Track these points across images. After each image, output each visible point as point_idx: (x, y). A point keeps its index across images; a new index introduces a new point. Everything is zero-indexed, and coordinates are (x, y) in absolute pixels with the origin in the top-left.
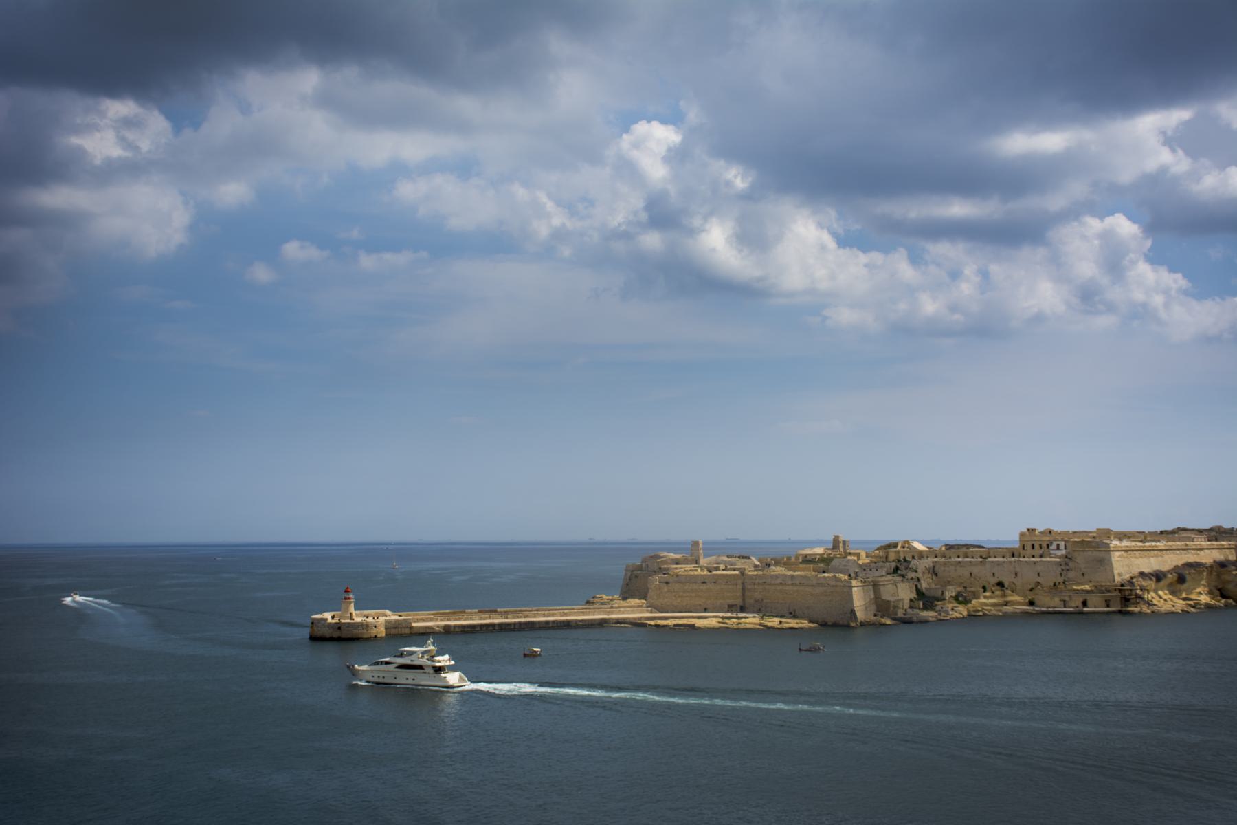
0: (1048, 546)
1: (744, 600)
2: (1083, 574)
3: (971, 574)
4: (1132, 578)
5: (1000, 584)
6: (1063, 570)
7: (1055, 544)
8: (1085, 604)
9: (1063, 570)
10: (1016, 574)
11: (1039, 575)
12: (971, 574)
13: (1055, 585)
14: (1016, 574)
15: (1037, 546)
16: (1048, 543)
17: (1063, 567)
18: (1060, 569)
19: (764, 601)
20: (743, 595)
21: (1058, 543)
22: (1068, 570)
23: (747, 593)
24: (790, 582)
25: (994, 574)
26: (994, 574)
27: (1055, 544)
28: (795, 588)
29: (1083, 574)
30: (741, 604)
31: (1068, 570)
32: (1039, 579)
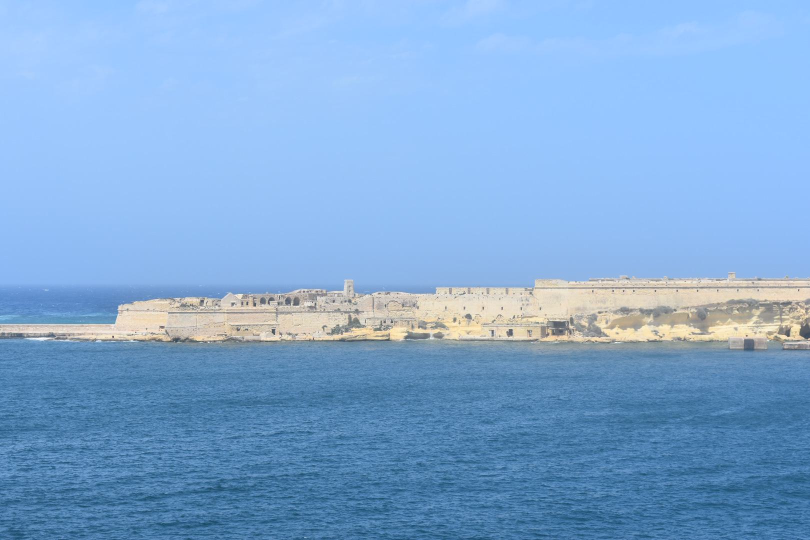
2: (540, 308)
3: (446, 307)
4: (600, 313)
5: (469, 317)
6: (523, 304)
8: (510, 333)
9: (523, 304)
10: (483, 308)
11: (502, 308)
12: (446, 307)
13: (514, 317)
14: (483, 308)
17: (524, 302)
18: (521, 304)
22: (528, 305)
25: (464, 308)
26: (464, 308)
29: (540, 308)
31: (528, 305)
32: (501, 312)
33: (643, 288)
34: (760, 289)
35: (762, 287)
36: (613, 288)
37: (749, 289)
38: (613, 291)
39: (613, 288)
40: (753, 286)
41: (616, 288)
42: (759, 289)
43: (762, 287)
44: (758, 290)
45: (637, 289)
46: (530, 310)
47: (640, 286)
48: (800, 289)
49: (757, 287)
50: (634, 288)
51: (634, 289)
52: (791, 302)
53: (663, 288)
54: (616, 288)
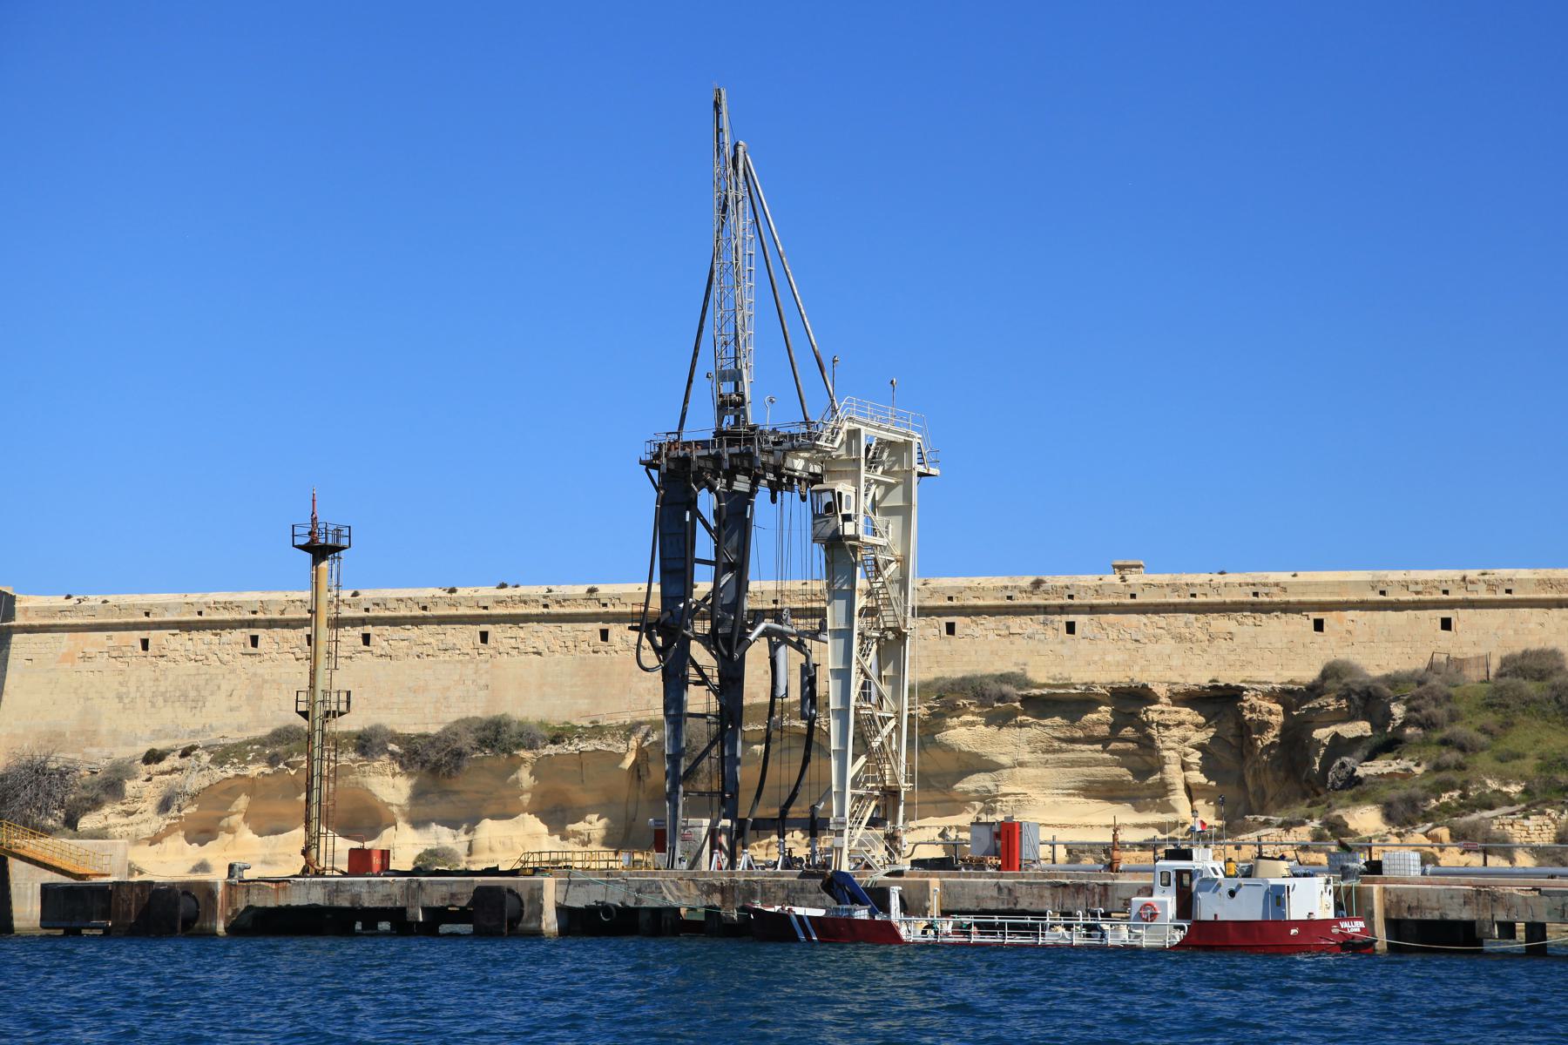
33: (416, 621)
34: (1080, 620)
35: (1093, 610)
36: (251, 624)
37: (1015, 623)
38: (254, 641)
39: (251, 624)
40: (1037, 600)
41: (271, 624)
42: (1071, 618)
43: (1093, 610)
44: (1071, 628)
45: (388, 631)
47: (403, 612)
48: (1329, 618)
49: (1062, 610)
50: (363, 622)
51: (369, 629)
52: (1240, 690)
53: (527, 618)
54: (271, 624)
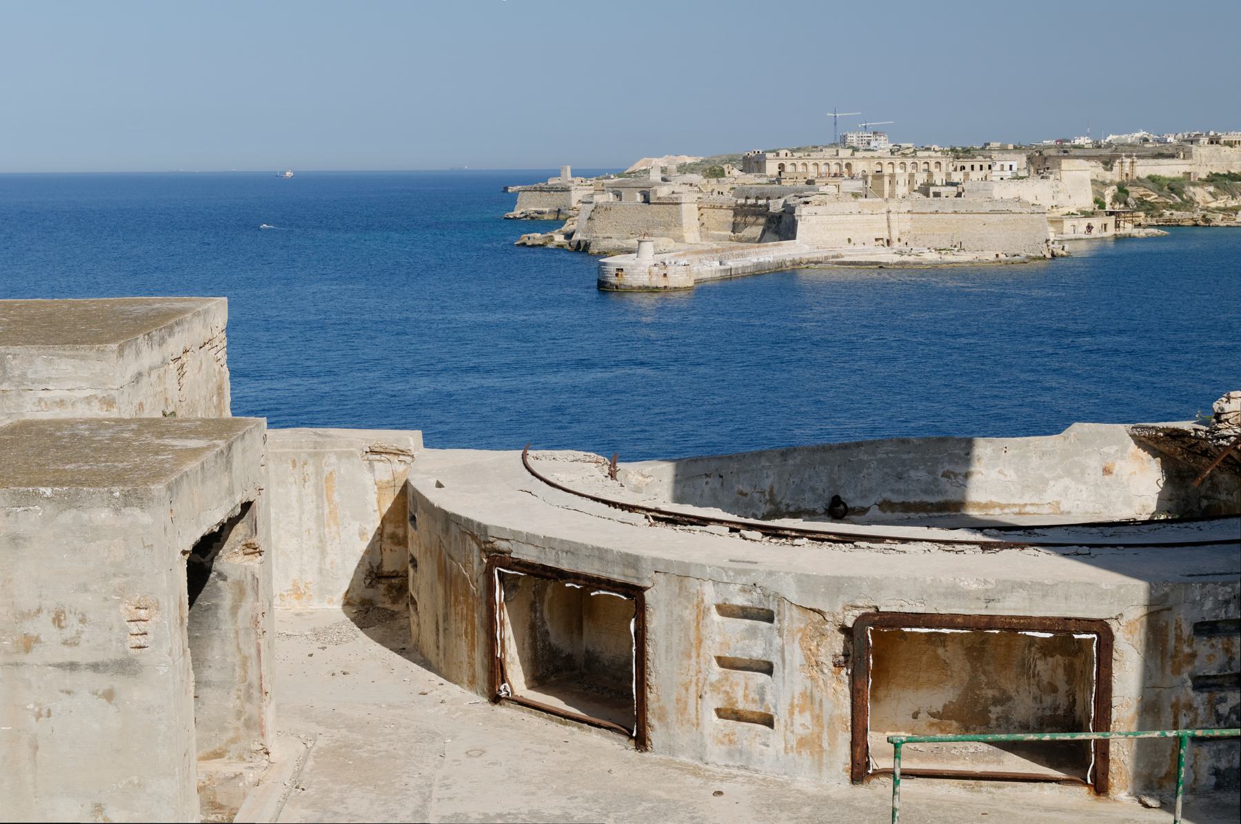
0: (990, 167)
1: (890, 232)
7: (999, 164)
15: (977, 167)
16: (990, 163)
19: (912, 233)
20: (889, 226)
21: (1002, 163)
22: (1058, 192)
23: (892, 225)
24: (951, 210)
27: (999, 164)
28: (959, 216)
30: (886, 237)
31: (1058, 192)
46: (1062, 198)
